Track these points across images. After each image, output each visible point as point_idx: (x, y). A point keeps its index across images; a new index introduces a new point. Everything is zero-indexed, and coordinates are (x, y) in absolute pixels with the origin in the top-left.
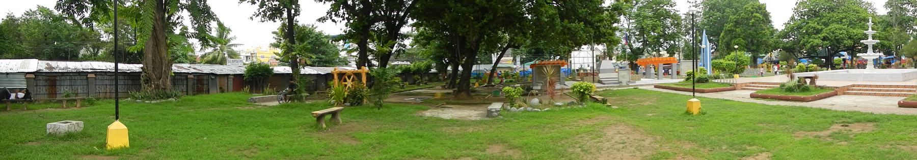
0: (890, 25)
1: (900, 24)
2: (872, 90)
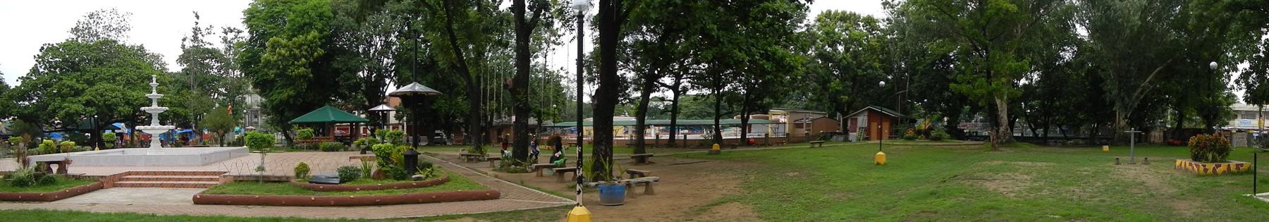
0: (186, 86)
1: (201, 85)
2: (157, 179)
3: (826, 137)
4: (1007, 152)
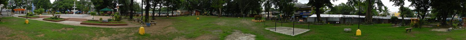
0: (80, 3)
1: (83, 3)
3: (188, 15)
4: (221, 18)
